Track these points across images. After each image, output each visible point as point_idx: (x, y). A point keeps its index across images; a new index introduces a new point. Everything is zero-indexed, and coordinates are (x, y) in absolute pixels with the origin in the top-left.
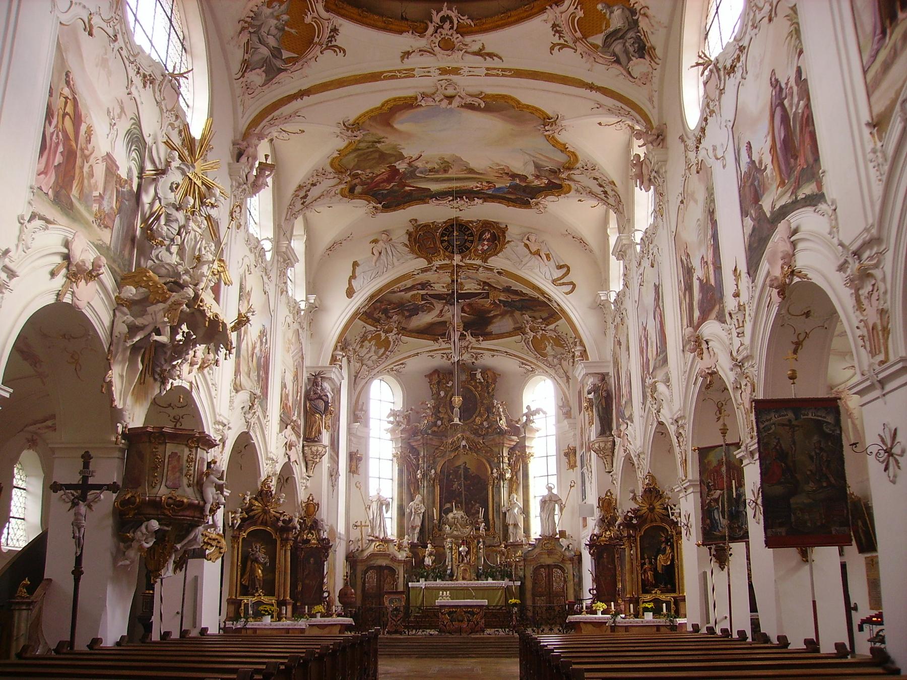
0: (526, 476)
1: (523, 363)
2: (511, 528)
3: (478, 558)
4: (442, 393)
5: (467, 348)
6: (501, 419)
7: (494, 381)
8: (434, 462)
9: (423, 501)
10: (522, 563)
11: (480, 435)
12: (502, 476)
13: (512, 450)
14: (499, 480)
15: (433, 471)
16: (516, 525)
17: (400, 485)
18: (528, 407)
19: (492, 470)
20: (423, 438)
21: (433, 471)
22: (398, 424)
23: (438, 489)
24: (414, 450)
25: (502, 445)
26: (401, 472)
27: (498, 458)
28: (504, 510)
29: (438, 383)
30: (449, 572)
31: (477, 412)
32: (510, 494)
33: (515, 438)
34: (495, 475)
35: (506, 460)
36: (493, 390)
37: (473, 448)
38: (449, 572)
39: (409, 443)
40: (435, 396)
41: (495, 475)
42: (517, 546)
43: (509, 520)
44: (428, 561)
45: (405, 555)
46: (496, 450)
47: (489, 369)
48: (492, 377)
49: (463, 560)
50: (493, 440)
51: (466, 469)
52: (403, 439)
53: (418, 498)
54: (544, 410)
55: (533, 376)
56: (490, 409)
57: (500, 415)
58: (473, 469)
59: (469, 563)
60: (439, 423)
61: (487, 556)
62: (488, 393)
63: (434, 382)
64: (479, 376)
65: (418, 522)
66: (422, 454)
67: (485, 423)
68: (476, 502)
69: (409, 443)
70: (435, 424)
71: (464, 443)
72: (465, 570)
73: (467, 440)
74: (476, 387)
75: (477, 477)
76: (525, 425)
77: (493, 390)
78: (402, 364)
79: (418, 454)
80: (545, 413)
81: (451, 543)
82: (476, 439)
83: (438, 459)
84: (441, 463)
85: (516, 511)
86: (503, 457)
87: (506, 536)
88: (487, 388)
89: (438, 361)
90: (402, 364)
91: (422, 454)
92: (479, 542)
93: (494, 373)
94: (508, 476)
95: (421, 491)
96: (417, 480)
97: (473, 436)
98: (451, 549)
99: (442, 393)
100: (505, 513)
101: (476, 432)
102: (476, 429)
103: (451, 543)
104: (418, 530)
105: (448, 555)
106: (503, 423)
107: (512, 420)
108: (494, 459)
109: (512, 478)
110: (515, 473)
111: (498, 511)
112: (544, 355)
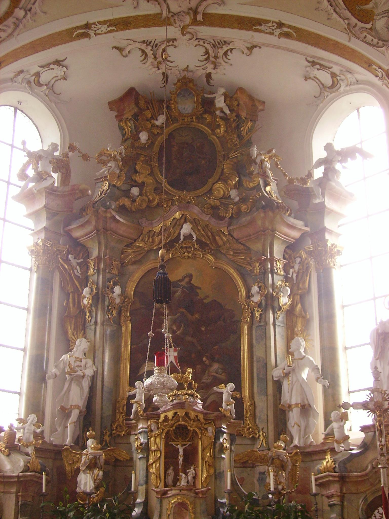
0: (326, 295)
1: (313, 63)
2: (294, 417)
3: (218, 476)
4: (144, 137)
5: (196, 12)
6: (267, 184)
7: (253, 115)
8: (121, 274)
9: (92, 353)
10: (334, 489)
11: (222, 218)
12: (270, 302)
13: (292, 248)
14: (265, 311)
15: (117, 290)
16: (306, 409)
17: (42, 311)
18: (328, 147)
19: (248, 290)
20: (96, 213)
21: (117, 290)
22: (41, 177)
23: (127, 329)
24: (78, 248)
25: (268, 234)
26: (45, 286)
27: (263, 264)
28: (276, 373)
29: (136, 117)
30: (137, 511)
31: (216, 176)
32: (290, 337)
33: (299, 224)
34: (256, 299)
35: (280, 265)
36: (250, 130)
37: (206, 243)
38: (137, 511)
39: (68, 234)
40: (129, 142)
41: (256, 299)
42: (311, 454)
43: (290, 396)
44: (86, 482)
45: (22, 464)
46: (256, 247)
47: (241, 90)
48: (246, 108)
49: (176, 480)
50: (252, 222)
51: (192, 289)
52: (51, 212)
53: (81, 345)
54: (366, 148)
55: (333, 100)
56: (244, 167)
57: (264, 176)
58: (206, 290)
59: (191, 487)
60: (135, 191)
61: (244, 463)
62: (240, 136)
63: (128, 115)
64: (220, 103)
65: (77, 397)
66: (95, 253)
67: (233, 193)
68: (212, 359)
69: (68, 234)
70: (127, 193)
71: (186, 229)
72: (181, 506)
73: (195, 223)
74: (214, 126)
75: (216, 305)
76: (323, 182)
77: (250, 130)
78: (58, 63)
79: (88, 256)
80: (365, 155)
81: (148, 432)
82: (213, 223)
83: (132, 268)
84: (137, 273)
85: (305, 374)
86: (272, 260)
87: (281, 427)
88: (238, 127)
89: (137, 73)
90: (58, 63)
91: (95, 253)
92: (219, 433)
93: (251, 98)
94: (284, 300)
95: (90, 334)
96: (82, 312)
97: (206, 218)
98: (146, 449)
99: (144, 137)
100: (278, 385)
101: (215, 212)
102: (214, 208)
103: (148, 432)
104: (75, 414)
105: (140, 465)
106: (271, 189)
107: (291, 181)
108: (254, 267)
109: (292, 307)
110: (299, 295)
111: (264, 380)
112: (366, 17)
